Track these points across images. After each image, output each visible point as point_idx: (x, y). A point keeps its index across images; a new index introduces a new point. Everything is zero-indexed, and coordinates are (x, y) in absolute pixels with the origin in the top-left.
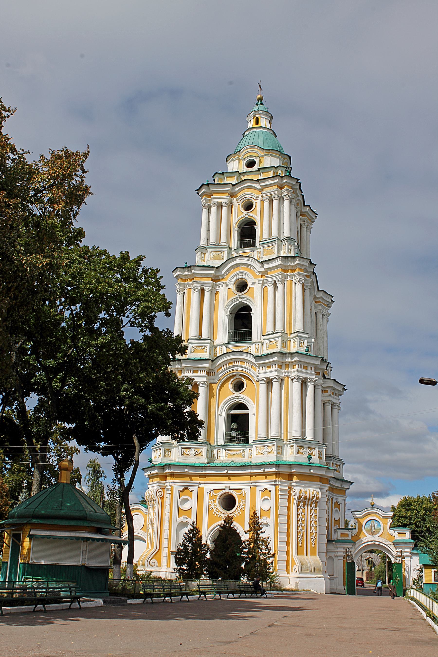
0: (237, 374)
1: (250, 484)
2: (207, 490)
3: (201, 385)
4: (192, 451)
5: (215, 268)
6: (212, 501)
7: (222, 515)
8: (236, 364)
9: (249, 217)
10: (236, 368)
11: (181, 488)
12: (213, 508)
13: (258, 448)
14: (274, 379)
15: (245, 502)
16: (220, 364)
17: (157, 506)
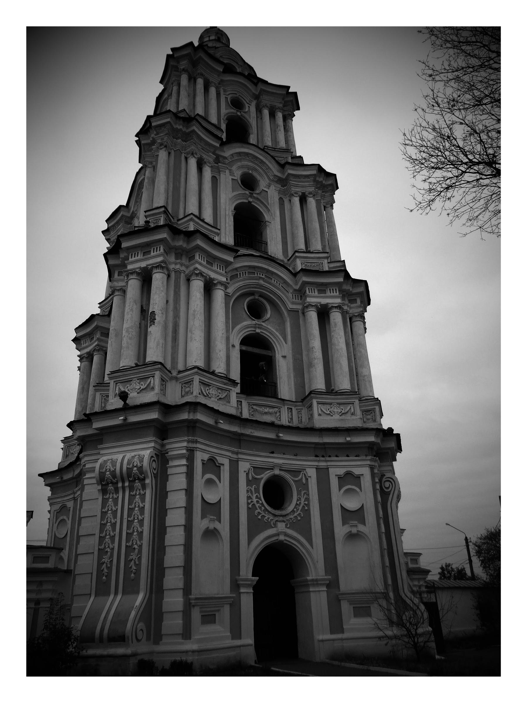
0: (258, 292)
1: (316, 463)
2: (244, 467)
3: (219, 287)
4: (213, 391)
5: (220, 142)
6: (253, 489)
7: (271, 517)
8: (261, 276)
9: (241, 117)
10: (261, 282)
11: (206, 457)
12: (256, 503)
13: (320, 406)
14: (336, 307)
15: (308, 495)
16: (236, 269)
17: (148, 492)
